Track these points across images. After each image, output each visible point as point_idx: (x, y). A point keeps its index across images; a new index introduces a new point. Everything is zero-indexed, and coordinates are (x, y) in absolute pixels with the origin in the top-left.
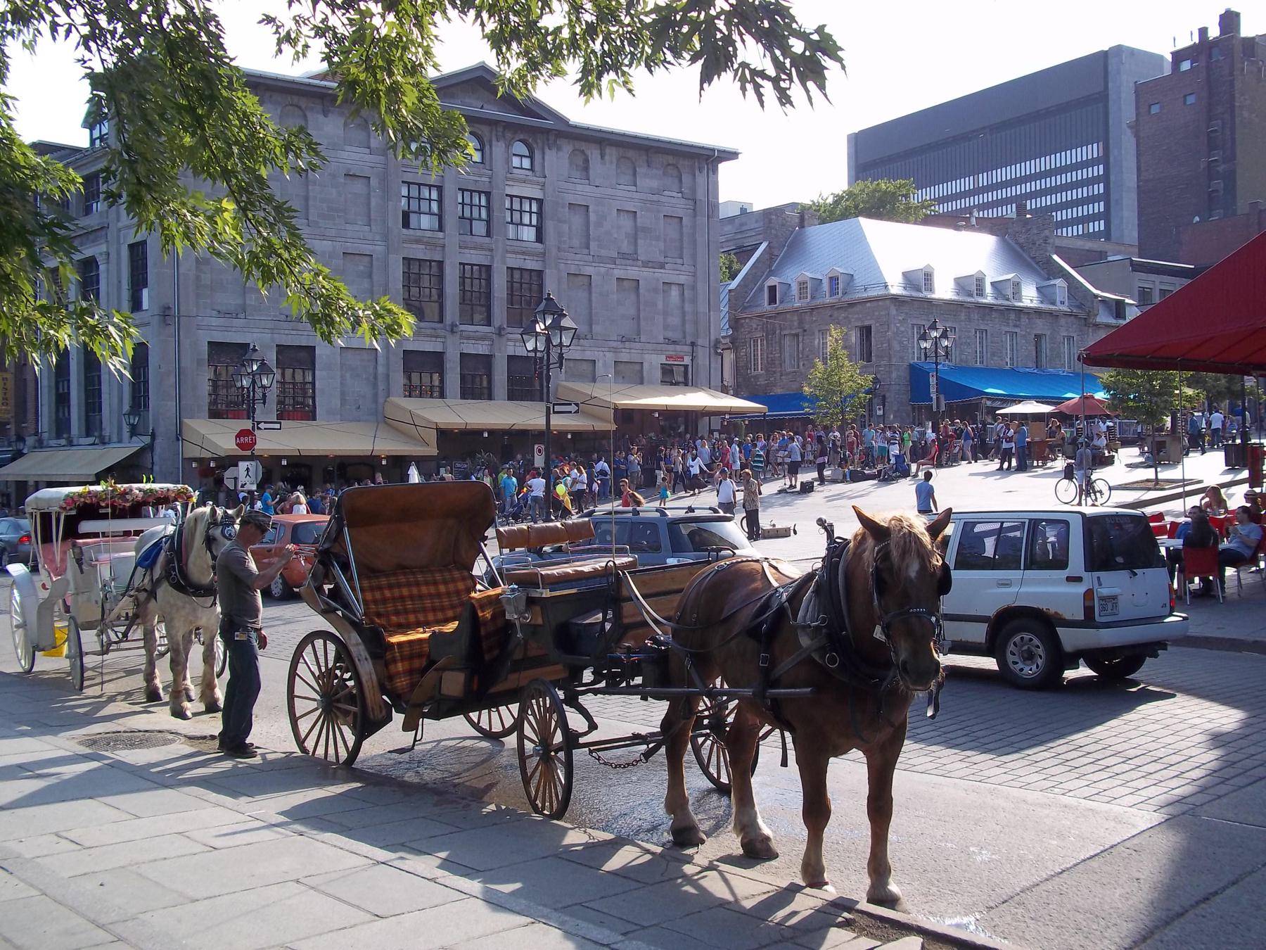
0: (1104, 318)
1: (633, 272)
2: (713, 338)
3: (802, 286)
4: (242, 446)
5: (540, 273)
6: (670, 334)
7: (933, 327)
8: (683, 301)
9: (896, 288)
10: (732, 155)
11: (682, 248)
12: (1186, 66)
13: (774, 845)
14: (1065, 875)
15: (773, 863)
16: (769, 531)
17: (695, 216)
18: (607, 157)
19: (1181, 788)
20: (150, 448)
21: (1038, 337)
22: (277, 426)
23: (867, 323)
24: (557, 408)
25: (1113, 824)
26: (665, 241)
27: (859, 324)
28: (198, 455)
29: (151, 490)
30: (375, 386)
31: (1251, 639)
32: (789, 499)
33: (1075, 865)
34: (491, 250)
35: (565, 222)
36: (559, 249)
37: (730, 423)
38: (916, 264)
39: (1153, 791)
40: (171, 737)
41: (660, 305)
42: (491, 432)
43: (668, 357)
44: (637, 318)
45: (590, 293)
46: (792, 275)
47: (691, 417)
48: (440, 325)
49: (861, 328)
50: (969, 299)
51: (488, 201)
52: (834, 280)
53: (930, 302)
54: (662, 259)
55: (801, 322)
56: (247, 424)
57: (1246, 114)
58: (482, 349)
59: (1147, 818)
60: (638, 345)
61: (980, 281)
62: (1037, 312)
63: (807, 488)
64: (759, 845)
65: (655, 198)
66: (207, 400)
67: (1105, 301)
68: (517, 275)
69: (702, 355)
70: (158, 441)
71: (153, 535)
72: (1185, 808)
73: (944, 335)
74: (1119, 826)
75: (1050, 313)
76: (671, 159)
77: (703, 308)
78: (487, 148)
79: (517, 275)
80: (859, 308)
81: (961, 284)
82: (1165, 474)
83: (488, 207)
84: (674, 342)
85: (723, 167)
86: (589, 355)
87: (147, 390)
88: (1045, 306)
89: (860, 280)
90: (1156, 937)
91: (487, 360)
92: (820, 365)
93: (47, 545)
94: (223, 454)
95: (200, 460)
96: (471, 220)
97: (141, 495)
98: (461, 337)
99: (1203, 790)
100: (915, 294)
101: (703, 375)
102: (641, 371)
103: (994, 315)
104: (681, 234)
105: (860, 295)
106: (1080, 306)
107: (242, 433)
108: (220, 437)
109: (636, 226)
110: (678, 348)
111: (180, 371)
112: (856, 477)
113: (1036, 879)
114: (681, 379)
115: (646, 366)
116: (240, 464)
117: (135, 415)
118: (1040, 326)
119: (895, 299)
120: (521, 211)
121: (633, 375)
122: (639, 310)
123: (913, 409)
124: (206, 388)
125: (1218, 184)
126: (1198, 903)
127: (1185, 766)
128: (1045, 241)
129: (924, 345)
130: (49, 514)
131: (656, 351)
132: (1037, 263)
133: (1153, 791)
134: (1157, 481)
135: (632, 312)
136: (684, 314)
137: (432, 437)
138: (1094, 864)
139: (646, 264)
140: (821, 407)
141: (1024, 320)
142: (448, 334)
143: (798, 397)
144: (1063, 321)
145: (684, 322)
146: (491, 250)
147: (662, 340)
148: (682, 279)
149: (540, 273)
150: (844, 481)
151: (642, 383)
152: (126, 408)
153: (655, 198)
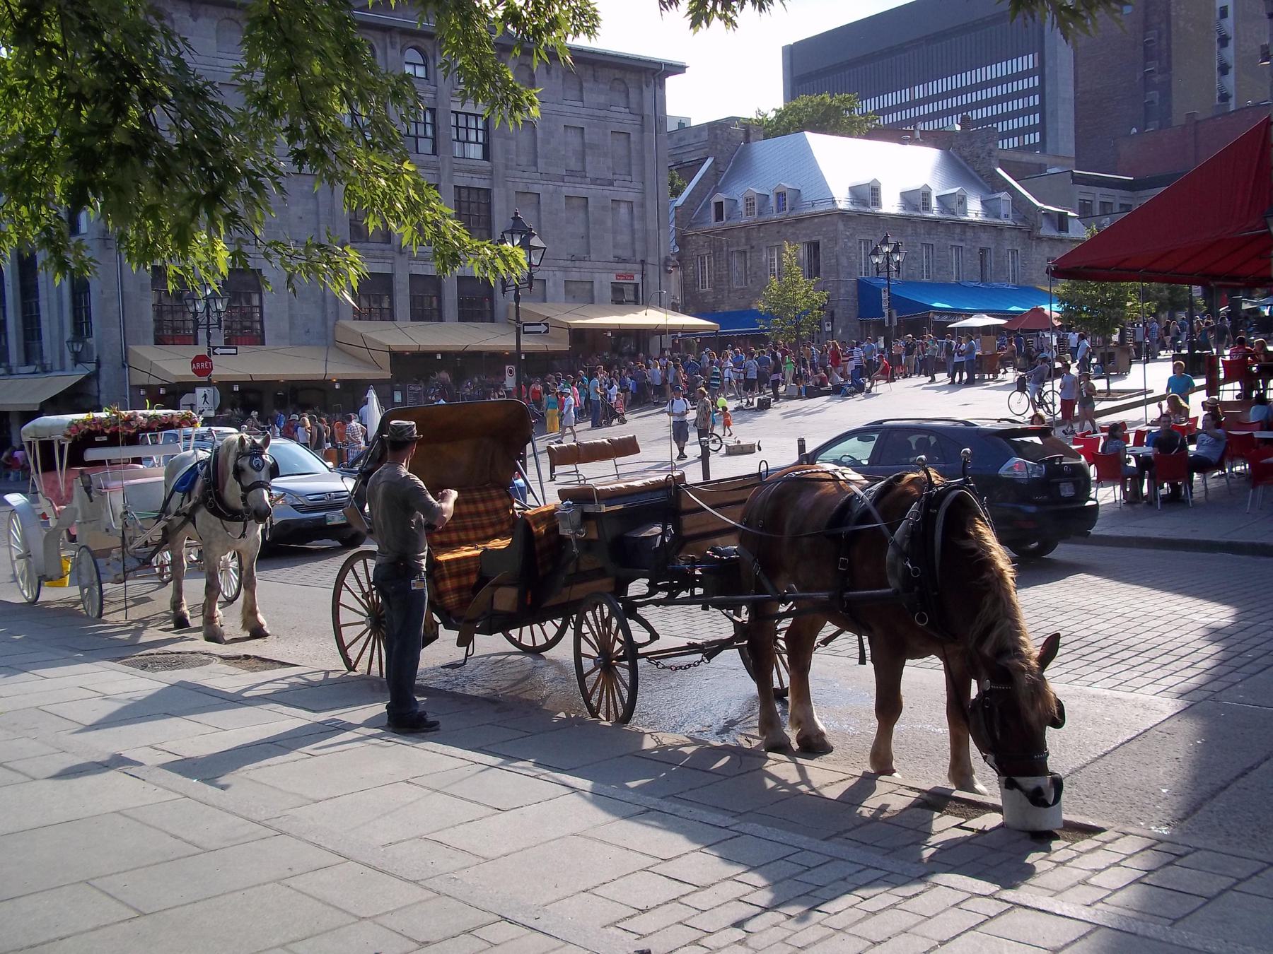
0: (1047, 231)
1: (582, 190)
2: (662, 256)
3: (749, 202)
4: (198, 372)
6: (620, 252)
7: (885, 242)
9: (843, 203)
10: (679, 69)
11: (630, 165)
13: (830, 740)
14: (1108, 757)
15: (829, 756)
16: (733, 447)
17: (642, 131)
18: (553, 72)
19: (1191, 678)
20: (95, 376)
21: (982, 250)
22: (234, 351)
23: (814, 239)
24: (527, 329)
25: (1141, 710)
26: (613, 157)
28: (146, 383)
29: (155, 416)
30: (324, 310)
31: (1226, 539)
32: (747, 415)
33: (1116, 748)
34: (438, 169)
35: (511, 139)
36: (507, 167)
38: (863, 178)
39: (1170, 681)
40: (205, 657)
41: (609, 223)
42: (444, 354)
46: (739, 191)
47: (641, 335)
48: (388, 246)
50: (916, 214)
51: (433, 118)
52: (781, 196)
53: (877, 217)
54: (610, 176)
55: (748, 239)
56: (202, 350)
57: (1182, 24)
59: (1169, 706)
60: (587, 264)
61: (925, 194)
62: (982, 225)
63: (764, 406)
64: (815, 741)
65: (602, 113)
66: (152, 326)
67: (1048, 214)
68: (464, 193)
69: (652, 273)
70: (104, 369)
71: (184, 460)
72: (1206, 694)
73: (896, 250)
74: (1148, 713)
75: (994, 227)
76: (618, 74)
77: (652, 226)
78: (431, 62)
79: (464, 193)
80: (804, 224)
81: (907, 198)
82: (1114, 386)
83: (434, 125)
84: (624, 261)
85: (670, 81)
87: (89, 316)
88: (988, 220)
89: (807, 196)
90: (1206, 808)
91: (435, 283)
92: (775, 283)
93: (50, 475)
94: (173, 381)
95: (147, 387)
96: (416, 137)
97: (146, 421)
99: (1215, 678)
100: (862, 209)
102: (592, 291)
103: (940, 229)
106: (1024, 220)
107: (198, 359)
108: (174, 364)
109: (584, 144)
111: (123, 297)
112: (811, 393)
113: (1081, 762)
114: (632, 298)
115: (596, 285)
116: (198, 390)
117: (78, 342)
118: (985, 240)
119: (843, 214)
120: (467, 128)
121: (585, 295)
123: (861, 323)
124: (150, 314)
125: (1154, 95)
126: (1237, 777)
127: (1194, 657)
128: (989, 154)
130: (51, 443)
132: (982, 176)
133: (1170, 681)
134: (1109, 391)
135: (582, 230)
136: (633, 232)
137: (385, 360)
138: (1133, 746)
139: (594, 181)
140: (775, 324)
141: (970, 234)
142: (396, 255)
143: (757, 314)
144: (1007, 234)
146: (438, 169)
147: (612, 259)
148: (631, 196)
150: (799, 397)
151: (592, 302)
152: (68, 335)
153: (602, 113)
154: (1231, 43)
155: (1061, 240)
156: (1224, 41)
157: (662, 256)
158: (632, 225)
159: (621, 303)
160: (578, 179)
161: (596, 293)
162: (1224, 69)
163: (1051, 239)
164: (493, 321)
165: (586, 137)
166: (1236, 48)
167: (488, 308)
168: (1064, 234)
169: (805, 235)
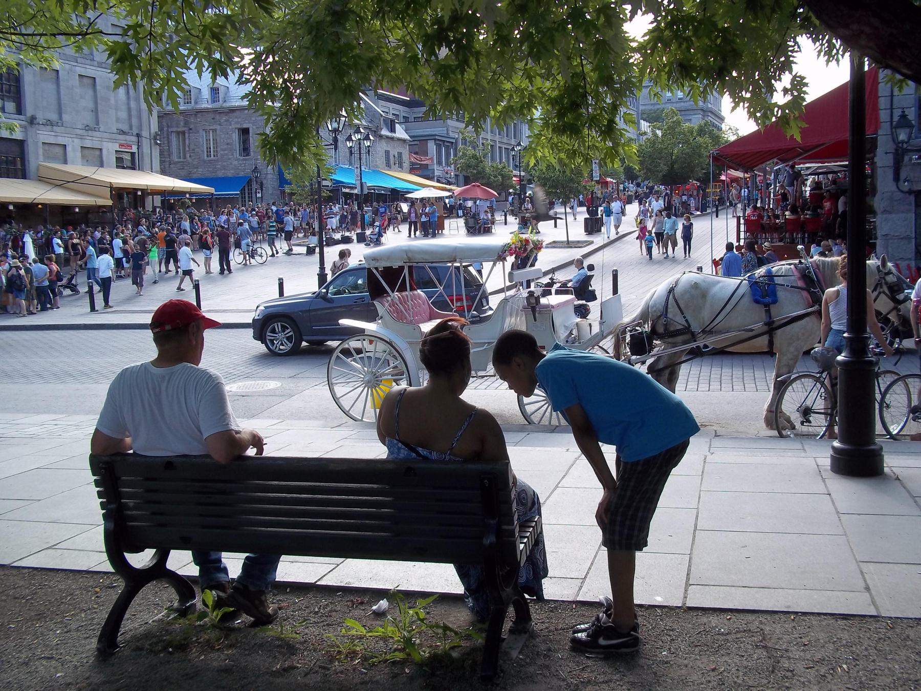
0: (385, 132)
2: (153, 131)
6: (121, 126)
23: (245, 126)
37: (201, 201)
43: (121, 145)
44: (95, 111)
49: (239, 129)
55: (186, 123)
60: (97, 134)
69: (146, 144)
80: (238, 113)
86: (61, 141)
101: (147, 160)
105: (233, 104)
110: (128, 138)
114: (129, 164)
115: (105, 152)
122: (96, 103)
129: (349, 144)
131: (113, 140)
135: (91, 105)
147: (115, 131)
151: (102, 165)
155: (392, 138)
158: (128, 104)
159: (123, 168)
160: (88, 62)
163: (387, 137)
164: (24, 176)
167: (19, 166)
168: (393, 135)
169: (237, 123)
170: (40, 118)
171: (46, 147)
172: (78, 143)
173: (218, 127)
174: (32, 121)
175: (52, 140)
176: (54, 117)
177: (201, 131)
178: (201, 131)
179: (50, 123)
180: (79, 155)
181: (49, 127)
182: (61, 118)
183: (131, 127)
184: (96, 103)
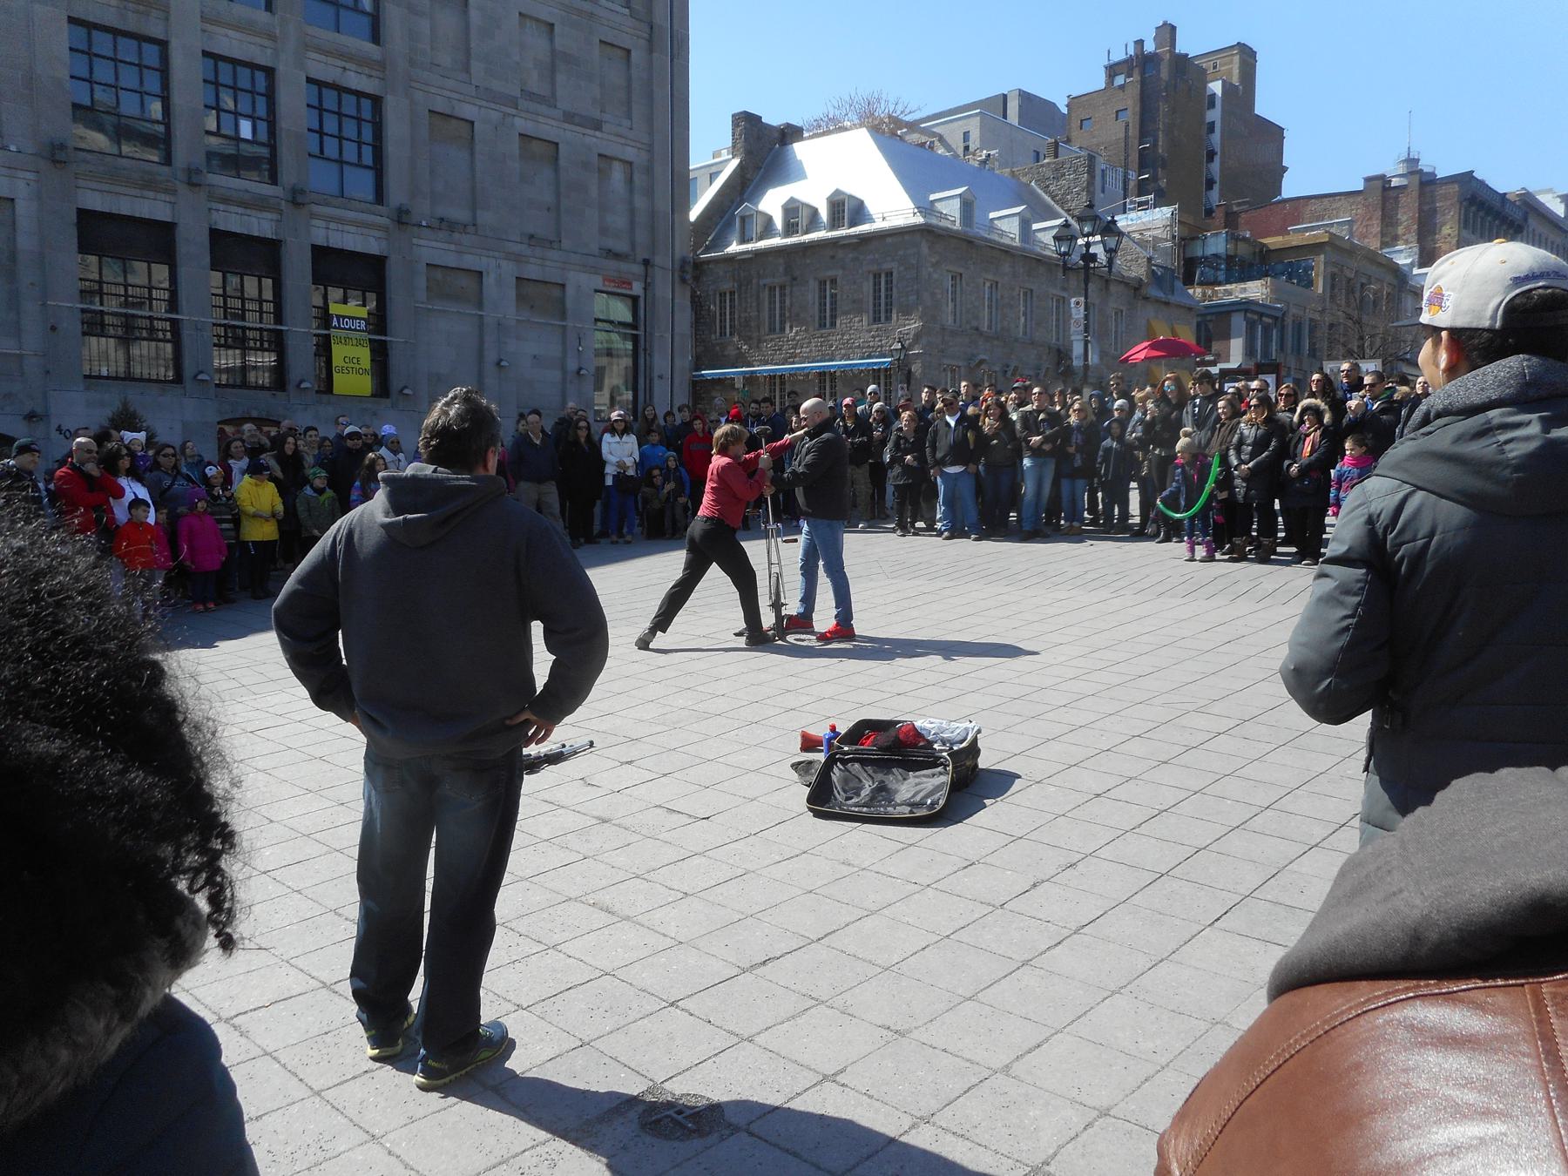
1: (548, 128)
2: (677, 256)
5: (377, 101)
6: (610, 243)
8: (631, 190)
11: (629, 102)
12: (1119, 80)
17: (651, 51)
23: (886, 266)
27: (875, 268)
34: (272, 37)
36: (412, 63)
45: (472, 154)
54: (596, 114)
58: (260, 225)
84: (617, 256)
86: (470, 261)
98: (211, 197)
102: (562, 301)
103: (1042, 269)
104: (629, 79)
109: (553, 51)
115: (570, 291)
136: (632, 212)
139: (569, 117)
142: (182, 189)
145: (632, 223)
146: (272, 37)
147: (596, 252)
148: (630, 153)
149: (377, 101)
154: (1217, 159)
155: (1167, 304)
156: (1211, 155)
157: (677, 256)
158: (631, 202)
160: (543, 109)
161: (569, 304)
162: (1210, 184)
163: (1158, 301)
165: (557, 40)
166: (1222, 163)
170: (423, 210)
171: (439, 275)
172: (509, 269)
173: (840, 272)
174: (402, 218)
175: (451, 261)
176: (459, 214)
177: (811, 282)
178: (811, 282)
179: (447, 225)
180: (512, 294)
181: (441, 235)
182: (474, 217)
183: (633, 245)
184: (558, 195)
